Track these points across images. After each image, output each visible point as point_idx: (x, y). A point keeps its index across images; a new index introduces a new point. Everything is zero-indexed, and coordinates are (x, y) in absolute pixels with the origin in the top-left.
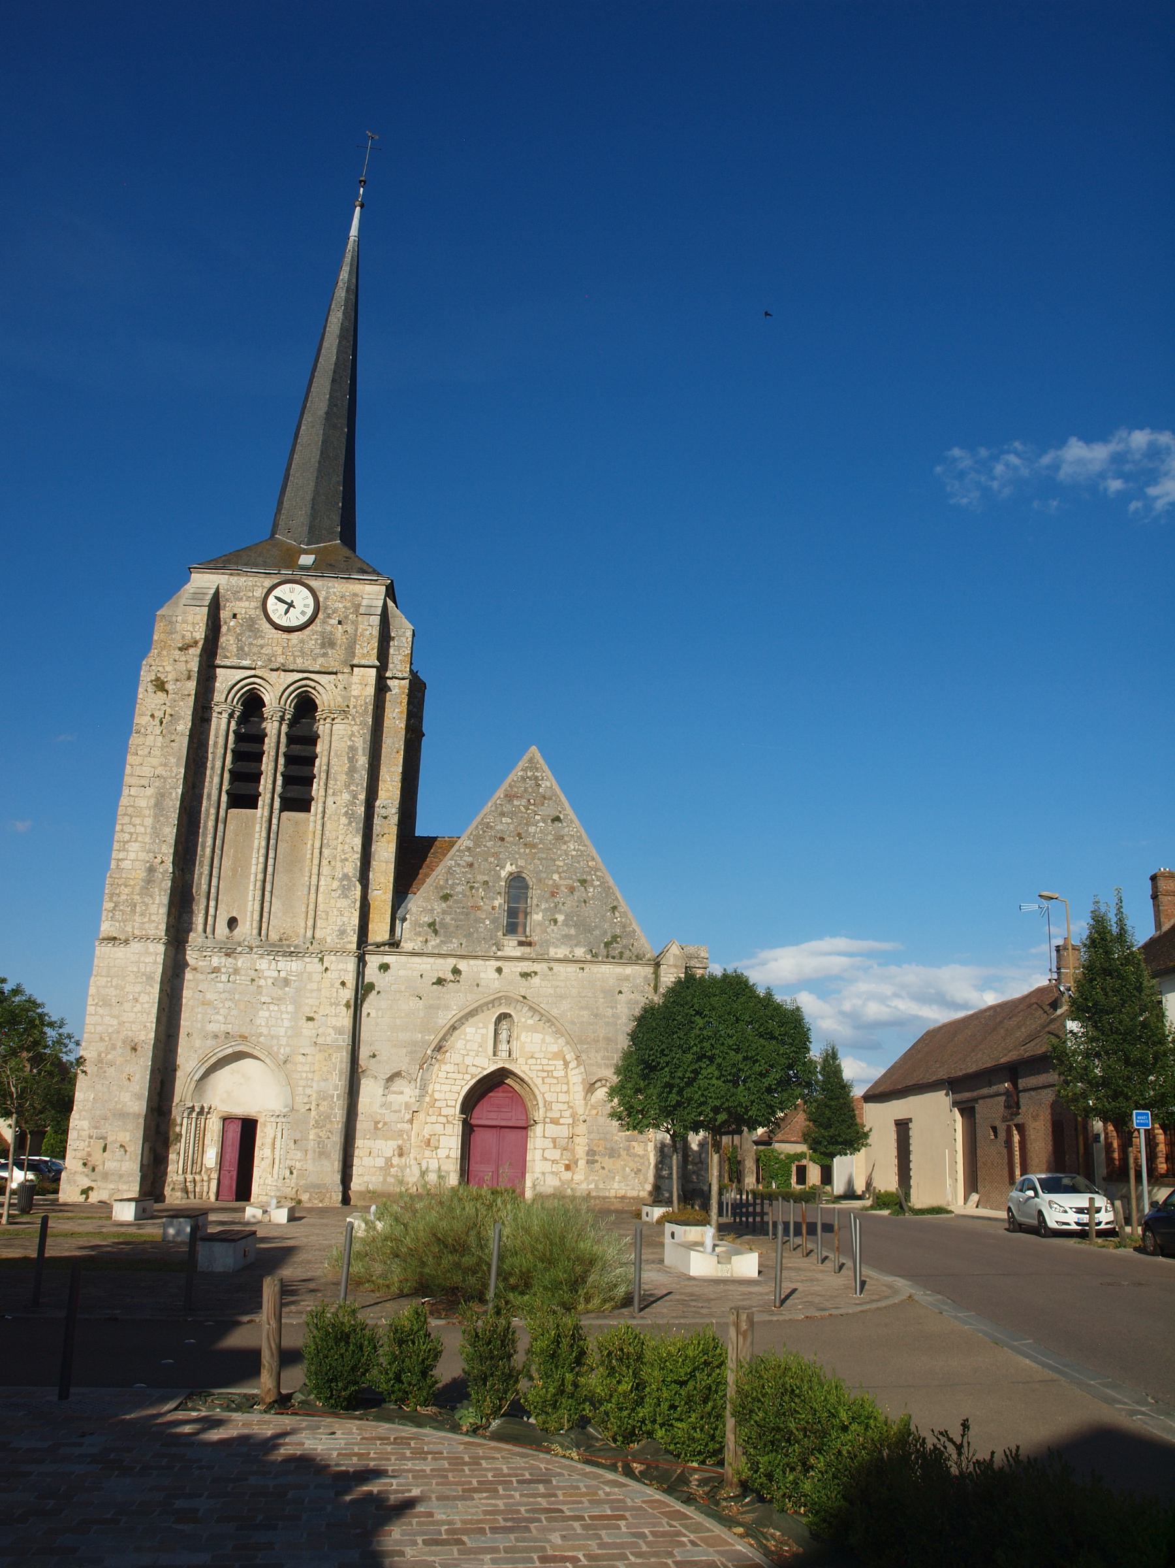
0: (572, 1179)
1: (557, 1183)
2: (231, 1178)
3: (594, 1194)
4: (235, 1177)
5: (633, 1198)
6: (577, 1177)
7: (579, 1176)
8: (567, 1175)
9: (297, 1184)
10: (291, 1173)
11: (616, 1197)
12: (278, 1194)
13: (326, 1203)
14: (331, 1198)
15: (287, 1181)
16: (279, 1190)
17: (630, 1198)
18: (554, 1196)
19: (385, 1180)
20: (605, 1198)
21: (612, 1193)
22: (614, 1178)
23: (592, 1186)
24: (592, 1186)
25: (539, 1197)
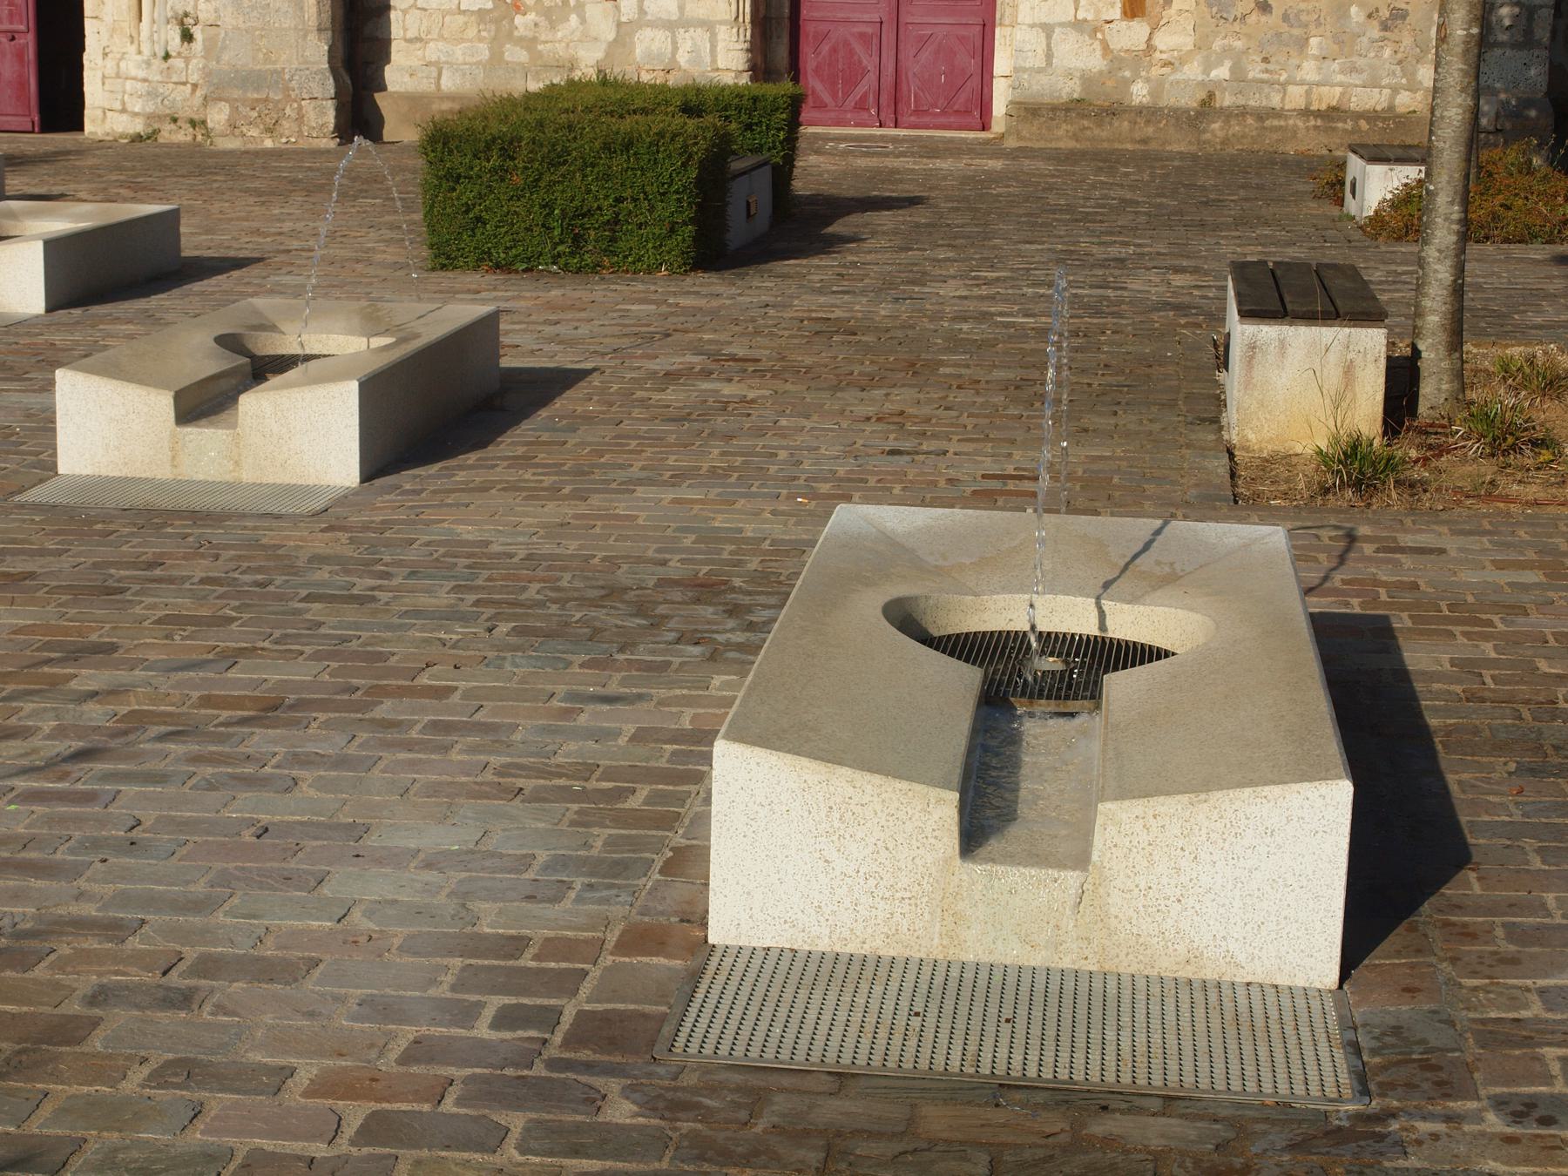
0: (1150, 48)
1: (1094, 62)
2: (20, 55)
3: (1226, 100)
4: (31, 54)
5: (1371, 116)
6: (1163, 41)
7: (1174, 38)
8: (1132, 35)
9: (207, 74)
10: (187, 37)
11: (1306, 113)
12: (150, 108)
13: (287, 137)
14: (300, 119)
15: (177, 63)
16: (152, 94)
17: (1358, 116)
18: (1074, 108)
19: (496, 57)
20: (1262, 115)
21: (1295, 97)
22: (1303, 43)
23: (1222, 72)
24: (1222, 72)
25: (1027, 110)
